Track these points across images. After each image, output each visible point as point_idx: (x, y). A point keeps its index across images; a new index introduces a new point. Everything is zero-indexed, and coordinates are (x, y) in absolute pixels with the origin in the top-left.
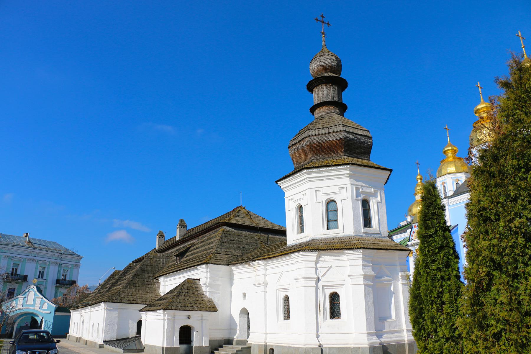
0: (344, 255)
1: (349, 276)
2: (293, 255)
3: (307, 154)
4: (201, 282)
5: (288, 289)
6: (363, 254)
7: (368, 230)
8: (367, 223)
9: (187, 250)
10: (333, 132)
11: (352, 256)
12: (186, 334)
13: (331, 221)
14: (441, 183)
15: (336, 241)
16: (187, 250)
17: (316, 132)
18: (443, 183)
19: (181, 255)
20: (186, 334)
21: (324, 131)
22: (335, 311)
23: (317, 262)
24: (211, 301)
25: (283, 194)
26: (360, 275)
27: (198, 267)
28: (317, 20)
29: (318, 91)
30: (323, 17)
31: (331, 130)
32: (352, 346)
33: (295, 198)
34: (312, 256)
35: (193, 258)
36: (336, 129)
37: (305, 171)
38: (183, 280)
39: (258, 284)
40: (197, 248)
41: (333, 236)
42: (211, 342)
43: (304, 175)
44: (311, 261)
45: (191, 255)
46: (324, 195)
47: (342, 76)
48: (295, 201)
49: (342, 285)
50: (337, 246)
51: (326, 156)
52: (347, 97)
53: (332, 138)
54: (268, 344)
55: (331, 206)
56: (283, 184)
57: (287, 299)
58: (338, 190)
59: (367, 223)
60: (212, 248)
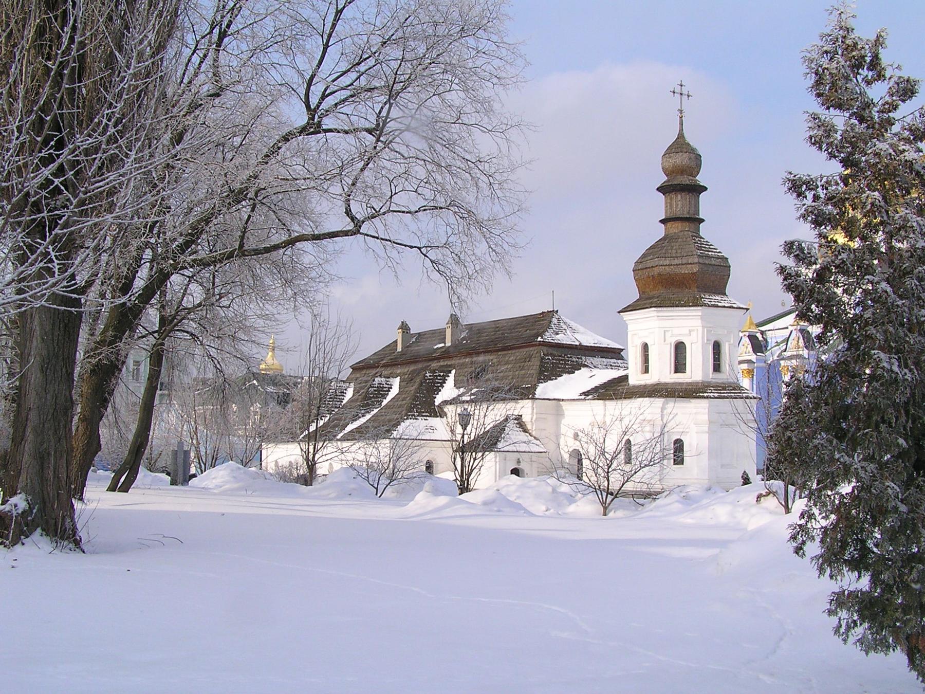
8: (717, 368)
17: (667, 262)
21: (676, 261)
23: (663, 409)
34: (659, 402)
41: (680, 381)
43: (652, 312)
46: (672, 336)
47: (701, 179)
51: (676, 290)
53: (685, 270)
55: (680, 348)
59: (717, 368)
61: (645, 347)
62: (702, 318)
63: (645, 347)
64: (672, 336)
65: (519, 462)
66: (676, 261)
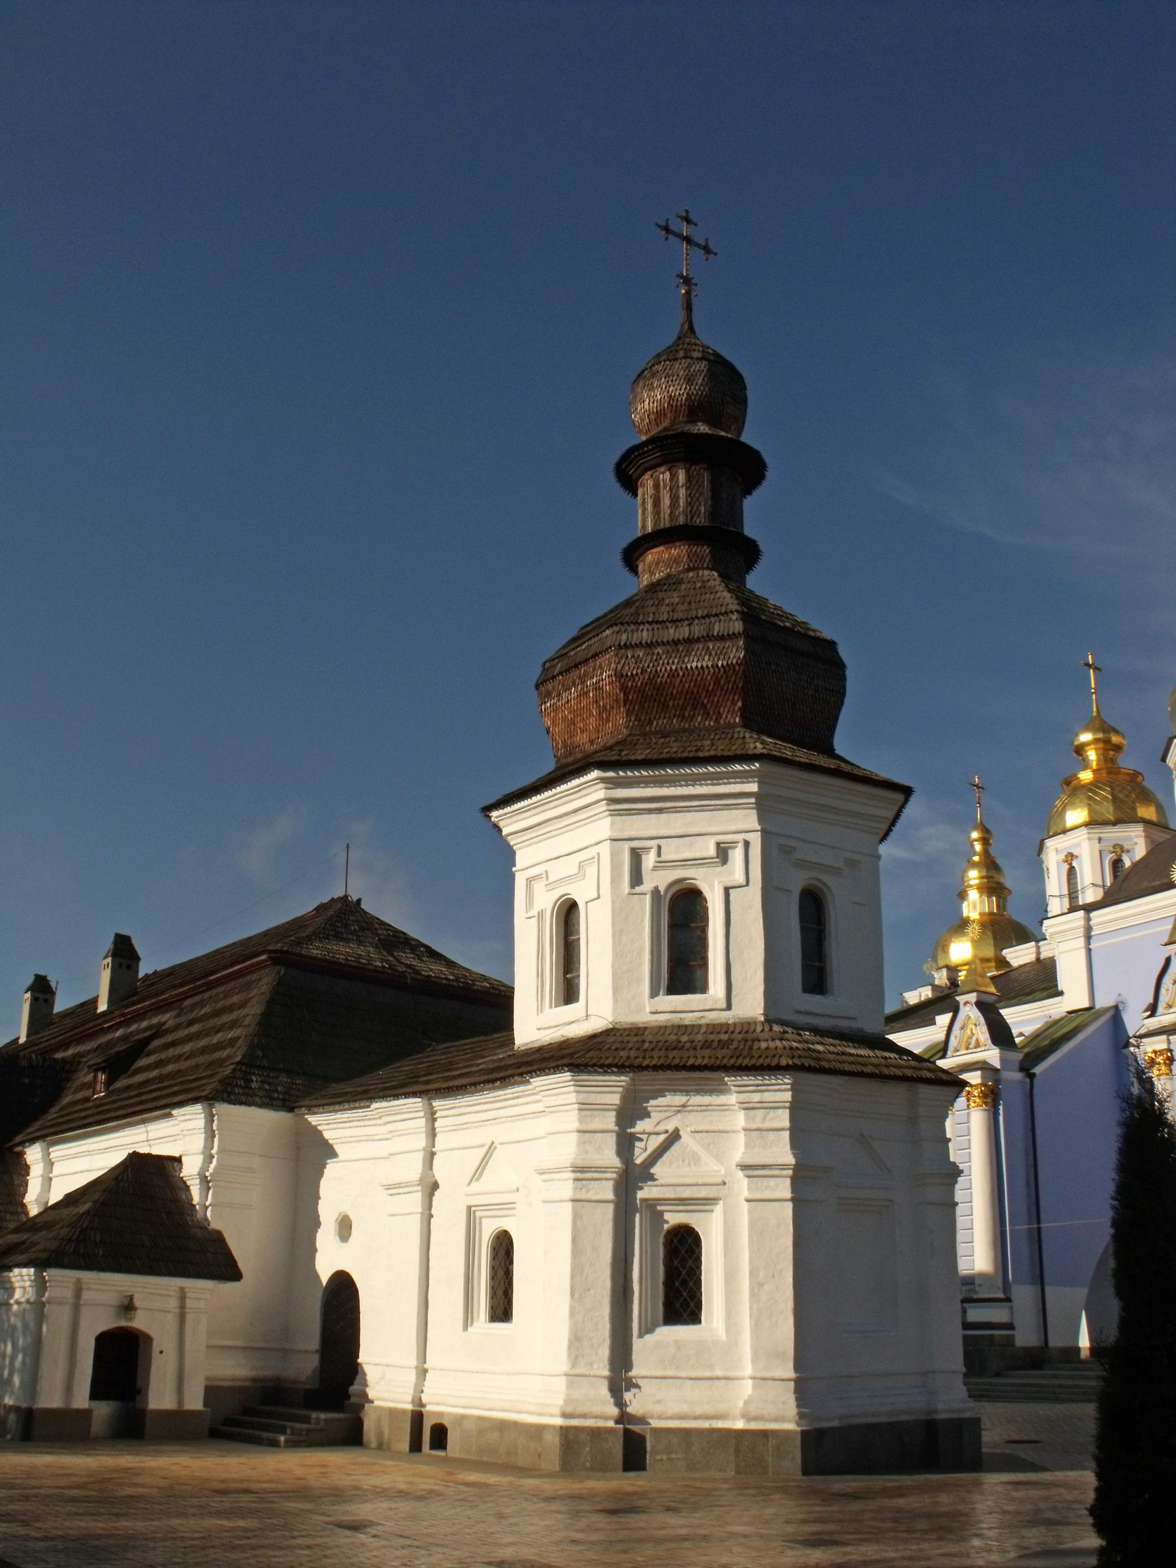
0: (722, 1090)
1: (744, 1167)
2: (538, 1082)
3: (604, 714)
4: (190, 1170)
5: (507, 1207)
6: (794, 1089)
7: (814, 1002)
8: (816, 978)
9: (139, 1048)
10: (709, 638)
11: (756, 1097)
12: (121, 1358)
13: (682, 966)
14: (1062, 856)
15: (700, 1037)
16: (139, 1048)
17: (645, 635)
18: (1070, 857)
19: (117, 1065)
20: (121, 1358)
21: (672, 633)
22: (682, 1300)
24: (218, 1239)
25: (509, 855)
26: (783, 1167)
27: (174, 1112)
28: (667, 229)
29: (656, 486)
30: (687, 220)
31: (698, 630)
32: (740, 1425)
33: (558, 870)
34: (610, 1090)
35: (161, 1078)
36: (717, 629)
37: (595, 774)
38: (116, 1158)
39: (398, 1185)
40: (173, 1044)
41: (688, 1019)
42: (212, 1392)
43: (589, 789)
44: (603, 1107)
45: (148, 1068)
46: (661, 865)
47: (748, 437)
48: (550, 886)
49: (711, 1201)
50: (704, 1057)
52: (756, 515)
54: (429, 1408)
55: (683, 913)
56: (512, 821)
57: (503, 1246)
58: (712, 851)
59: (816, 978)
60: (232, 1042)
61: (568, 912)
62: (764, 805)
63: (568, 912)
64: (661, 865)
65: (128, 1307)
66: (672, 633)
